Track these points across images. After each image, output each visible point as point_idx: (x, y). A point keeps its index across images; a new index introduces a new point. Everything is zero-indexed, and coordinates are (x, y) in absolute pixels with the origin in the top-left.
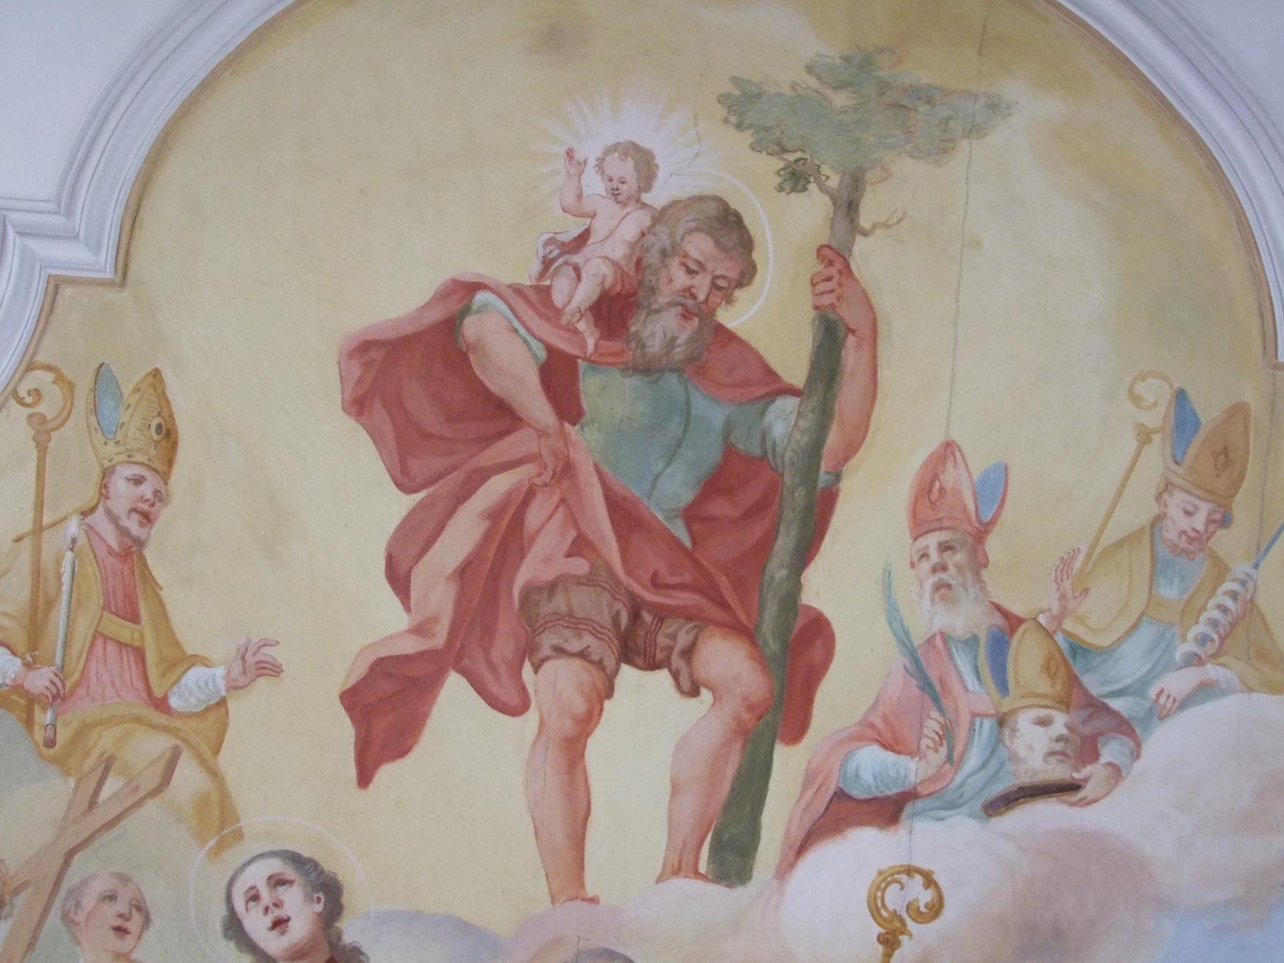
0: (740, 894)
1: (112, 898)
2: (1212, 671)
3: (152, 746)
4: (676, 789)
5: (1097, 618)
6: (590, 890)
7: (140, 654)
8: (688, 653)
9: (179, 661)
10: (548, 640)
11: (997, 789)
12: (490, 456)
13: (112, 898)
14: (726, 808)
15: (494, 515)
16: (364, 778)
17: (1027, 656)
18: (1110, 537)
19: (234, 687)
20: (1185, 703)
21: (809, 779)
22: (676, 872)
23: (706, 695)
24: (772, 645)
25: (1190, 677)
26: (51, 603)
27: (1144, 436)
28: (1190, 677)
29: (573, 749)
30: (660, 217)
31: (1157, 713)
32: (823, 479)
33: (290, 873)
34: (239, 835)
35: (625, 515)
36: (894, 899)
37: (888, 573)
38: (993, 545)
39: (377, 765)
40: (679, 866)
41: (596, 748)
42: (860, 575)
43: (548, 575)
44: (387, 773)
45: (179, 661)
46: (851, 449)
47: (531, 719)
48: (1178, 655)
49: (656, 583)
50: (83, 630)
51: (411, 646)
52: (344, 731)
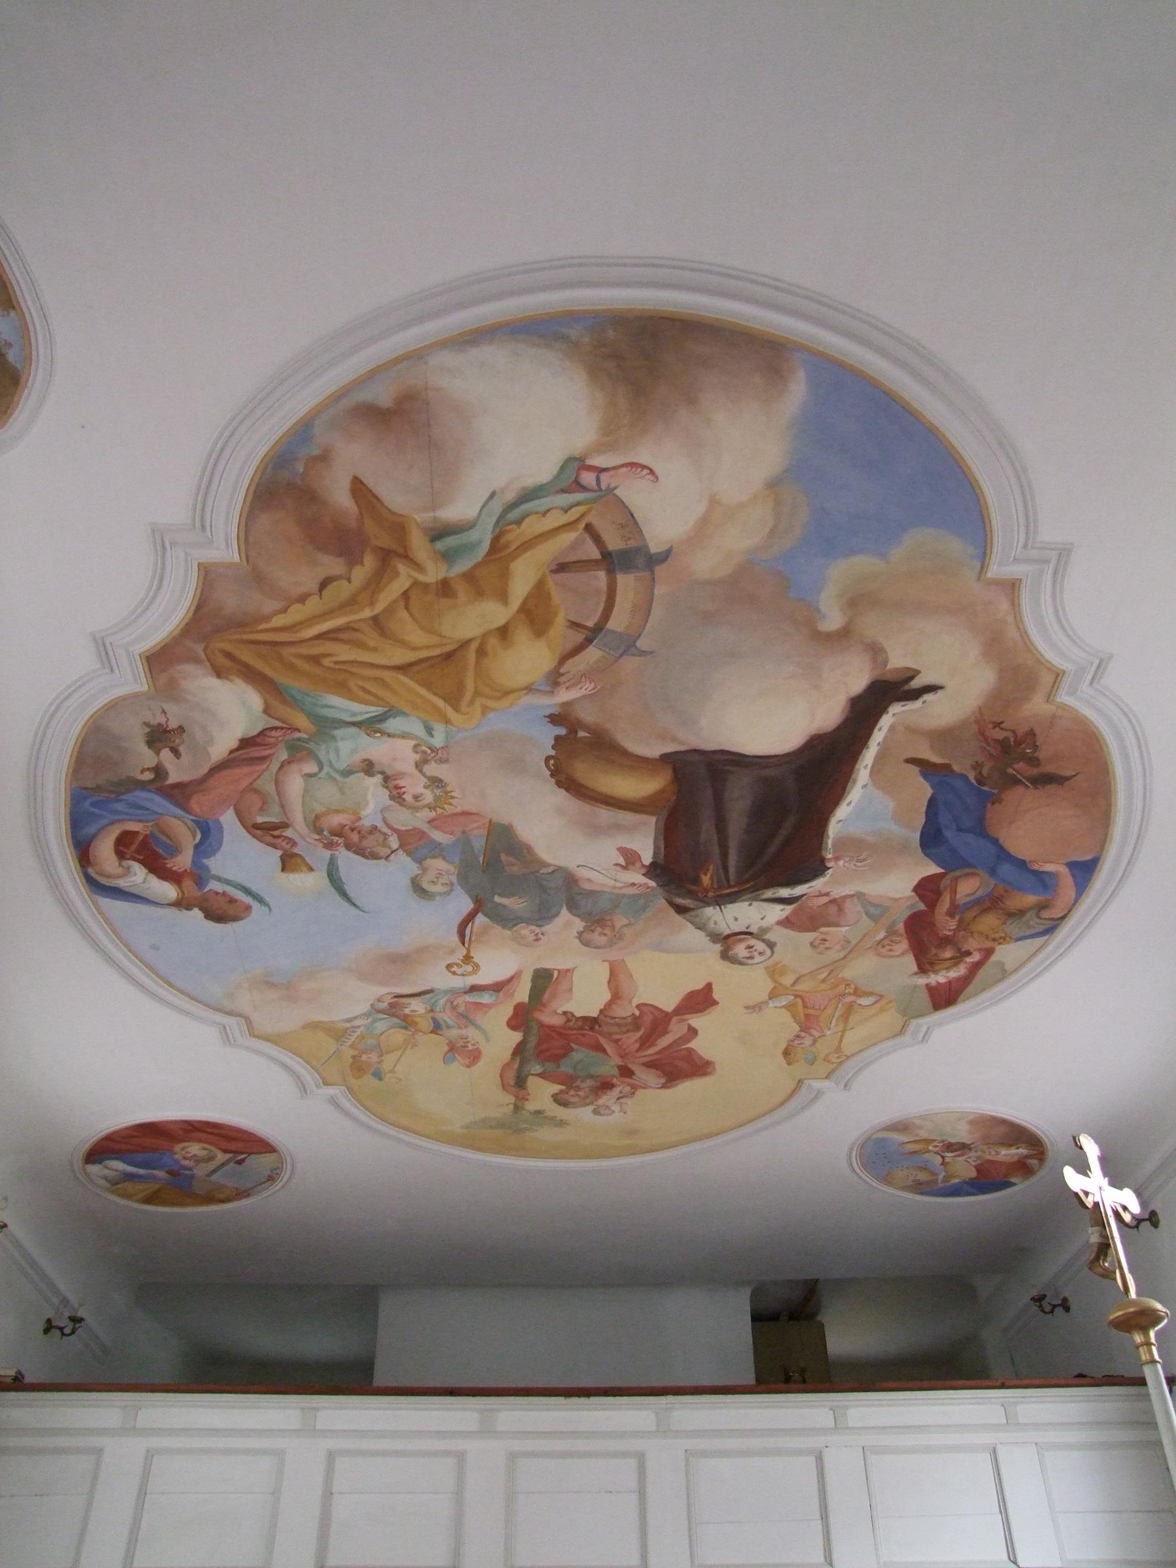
0: (539, 966)
1: (827, 948)
2: (348, 1025)
3: (802, 987)
4: (571, 990)
5: (399, 1036)
6: (607, 965)
7: (805, 1006)
8: (569, 1020)
9: (789, 1007)
10: (629, 1020)
11: (428, 996)
12: (655, 1057)
13: (827, 948)
14: (546, 987)
15: (653, 1045)
16: (709, 987)
17: (425, 1024)
18: (399, 1053)
19: (767, 1003)
20: (356, 1018)
21: (512, 995)
22: (568, 970)
23: (560, 1011)
24: (534, 1024)
25: (356, 1023)
26: (841, 1016)
27: (392, 1071)
28: (356, 1023)
29: (616, 996)
30: (592, 1103)
31: (367, 1015)
32: (518, 1059)
33: (745, 961)
34: (766, 968)
35: (599, 1048)
36: (469, 968)
37: (487, 1040)
38: (446, 1048)
39: (703, 989)
40: (566, 973)
41: (607, 996)
42: (498, 1039)
43: (630, 1034)
44: (699, 985)
45: (789, 1007)
46: (507, 1066)
47: (635, 1002)
48: (362, 1029)
49: (584, 1035)
50: (829, 1011)
51: (686, 1017)
52: (716, 995)
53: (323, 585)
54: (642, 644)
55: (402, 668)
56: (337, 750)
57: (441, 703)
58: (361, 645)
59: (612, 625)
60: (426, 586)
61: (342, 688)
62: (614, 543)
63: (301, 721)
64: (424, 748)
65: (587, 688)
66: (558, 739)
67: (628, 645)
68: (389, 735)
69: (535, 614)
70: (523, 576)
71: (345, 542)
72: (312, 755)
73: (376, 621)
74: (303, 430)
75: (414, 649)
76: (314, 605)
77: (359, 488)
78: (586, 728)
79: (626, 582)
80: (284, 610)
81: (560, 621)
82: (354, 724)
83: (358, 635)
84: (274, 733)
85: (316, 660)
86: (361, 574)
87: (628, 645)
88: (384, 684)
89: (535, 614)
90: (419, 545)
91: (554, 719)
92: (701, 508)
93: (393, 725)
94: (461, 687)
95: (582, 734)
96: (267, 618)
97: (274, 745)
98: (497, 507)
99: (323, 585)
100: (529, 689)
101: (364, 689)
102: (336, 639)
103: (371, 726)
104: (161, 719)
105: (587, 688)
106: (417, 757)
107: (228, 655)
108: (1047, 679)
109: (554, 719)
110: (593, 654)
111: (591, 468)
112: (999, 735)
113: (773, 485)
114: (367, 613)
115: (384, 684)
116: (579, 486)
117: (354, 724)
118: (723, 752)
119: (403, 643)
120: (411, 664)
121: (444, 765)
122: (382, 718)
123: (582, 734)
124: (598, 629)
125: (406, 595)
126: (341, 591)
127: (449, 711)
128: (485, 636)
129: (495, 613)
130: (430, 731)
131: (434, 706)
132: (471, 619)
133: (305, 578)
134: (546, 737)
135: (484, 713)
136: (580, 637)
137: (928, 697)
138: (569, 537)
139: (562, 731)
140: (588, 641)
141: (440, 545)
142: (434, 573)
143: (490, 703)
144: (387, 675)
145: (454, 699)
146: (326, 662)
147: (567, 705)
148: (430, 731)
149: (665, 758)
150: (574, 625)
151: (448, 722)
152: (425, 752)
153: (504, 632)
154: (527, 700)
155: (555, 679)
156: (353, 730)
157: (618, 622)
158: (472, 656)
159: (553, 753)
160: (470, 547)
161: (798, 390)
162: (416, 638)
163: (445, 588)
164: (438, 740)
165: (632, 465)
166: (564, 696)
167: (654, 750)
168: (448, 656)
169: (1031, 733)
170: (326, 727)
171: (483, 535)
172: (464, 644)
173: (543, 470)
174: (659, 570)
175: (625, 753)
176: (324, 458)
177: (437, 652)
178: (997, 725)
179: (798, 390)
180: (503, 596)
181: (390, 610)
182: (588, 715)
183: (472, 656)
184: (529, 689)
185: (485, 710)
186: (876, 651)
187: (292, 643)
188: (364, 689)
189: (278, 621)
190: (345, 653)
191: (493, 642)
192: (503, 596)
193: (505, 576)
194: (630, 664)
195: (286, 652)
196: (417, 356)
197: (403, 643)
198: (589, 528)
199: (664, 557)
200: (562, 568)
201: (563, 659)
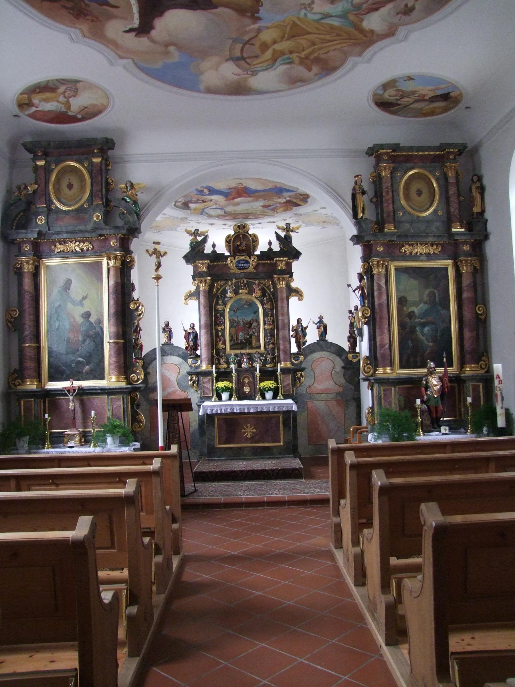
53: (328, 52)
54: (232, 41)
55: (310, 33)
56: (343, 7)
57: (299, 23)
58: (321, 39)
59: (241, 45)
60: (297, 52)
61: (332, 27)
62: (243, 62)
63: (352, 17)
64: (309, 9)
65: (248, 29)
66: (258, 13)
67: (235, 41)
68: (321, 13)
69: (265, 47)
70: (269, 54)
71: (317, 60)
72: (353, 5)
73: (314, 44)
74: (320, 78)
75: (304, 39)
76: (332, 48)
77: (310, 70)
78: (248, 17)
79: (238, 54)
80: (342, 47)
81: (257, 46)
82: (332, 16)
83: (321, 41)
84: (363, 13)
85: (338, 35)
86: (316, 55)
87: (235, 41)
88: (317, 29)
89: (265, 47)
90: (297, 60)
91: (259, 19)
92: (219, 69)
93: (318, 17)
94: (291, 28)
95: (249, 14)
96: (349, 45)
97: (366, 9)
98: (274, 67)
99: (328, 52)
100: (268, 28)
101: (325, 27)
102: (328, 40)
103: (327, 16)
104: (403, 17)
105: (248, 29)
106: (313, 6)
107: (365, 36)
108: (87, 34)
109: (259, 19)
110: (247, 38)
111: (250, 74)
112: (88, 17)
113: (202, 73)
114: (316, 47)
115: (317, 29)
116: (253, 72)
117: (332, 16)
118: (194, 10)
119: (307, 39)
120: (306, 34)
121: (302, 2)
122: (321, 19)
123: (249, 14)
124: (245, 44)
125: (303, 50)
126: (322, 52)
127: (297, 21)
128: (281, 41)
129: (277, 47)
130: (305, 15)
131: (302, 23)
132: (285, 45)
133: (331, 54)
134: (263, 13)
135: (285, 20)
136: (251, 42)
137: (127, 29)
138: (254, 63)
139: (256, 15)
140: (248, 41)
141: (291, 60)
142: (294, 55)
143: (281, 23)
144: (316, 31)
145: (294, 24)
146: (335, 34)
147: (254, 23)
148: (305, 15)
149: (216, 7)
150: (253, 45)
151: (299, 19)
152: (309, 8)
153: (275, 42)
154: (269, 25)
155: (259, 31)
156: (334, 14)
157: (239, 46)
158: (286, 36)
159: (260, 8)
160: (284, 60)
161: (202, 87)
162: (303, 41)
163: (291, 52)
164: (303, 12)
165: (240, 75)
166: (256, 26)
167: (220, 10)
168: (294, 36)
169: (78, 19)
170: (344, 16)
171: (278, 62)
172: (288, 39)
173: (261, 74)
174: (229, 57)
175: (230, 8)
176: (316, 75)
177: (297, 38)
178: (92, 21)
179: (202, 87)
180: (274, 51)
181: (309, 47)
182: (247, 21)
183: (286, 36)
184: (268, 28)
185: (284, 21)
186: (153, 41)
187: (343, 39)
188: (325, 27)
189: (345, 45)
190: (328, 37)
191: (279, 40)
192: (274, 51)
193: (273, 55)
194: (234, 36)
195: (347, 37)
196: (289, 89)
197: (307, 39)
198: (250, 65)
199: (227, 60)
200: (257, 57)
201: (256, 36)
